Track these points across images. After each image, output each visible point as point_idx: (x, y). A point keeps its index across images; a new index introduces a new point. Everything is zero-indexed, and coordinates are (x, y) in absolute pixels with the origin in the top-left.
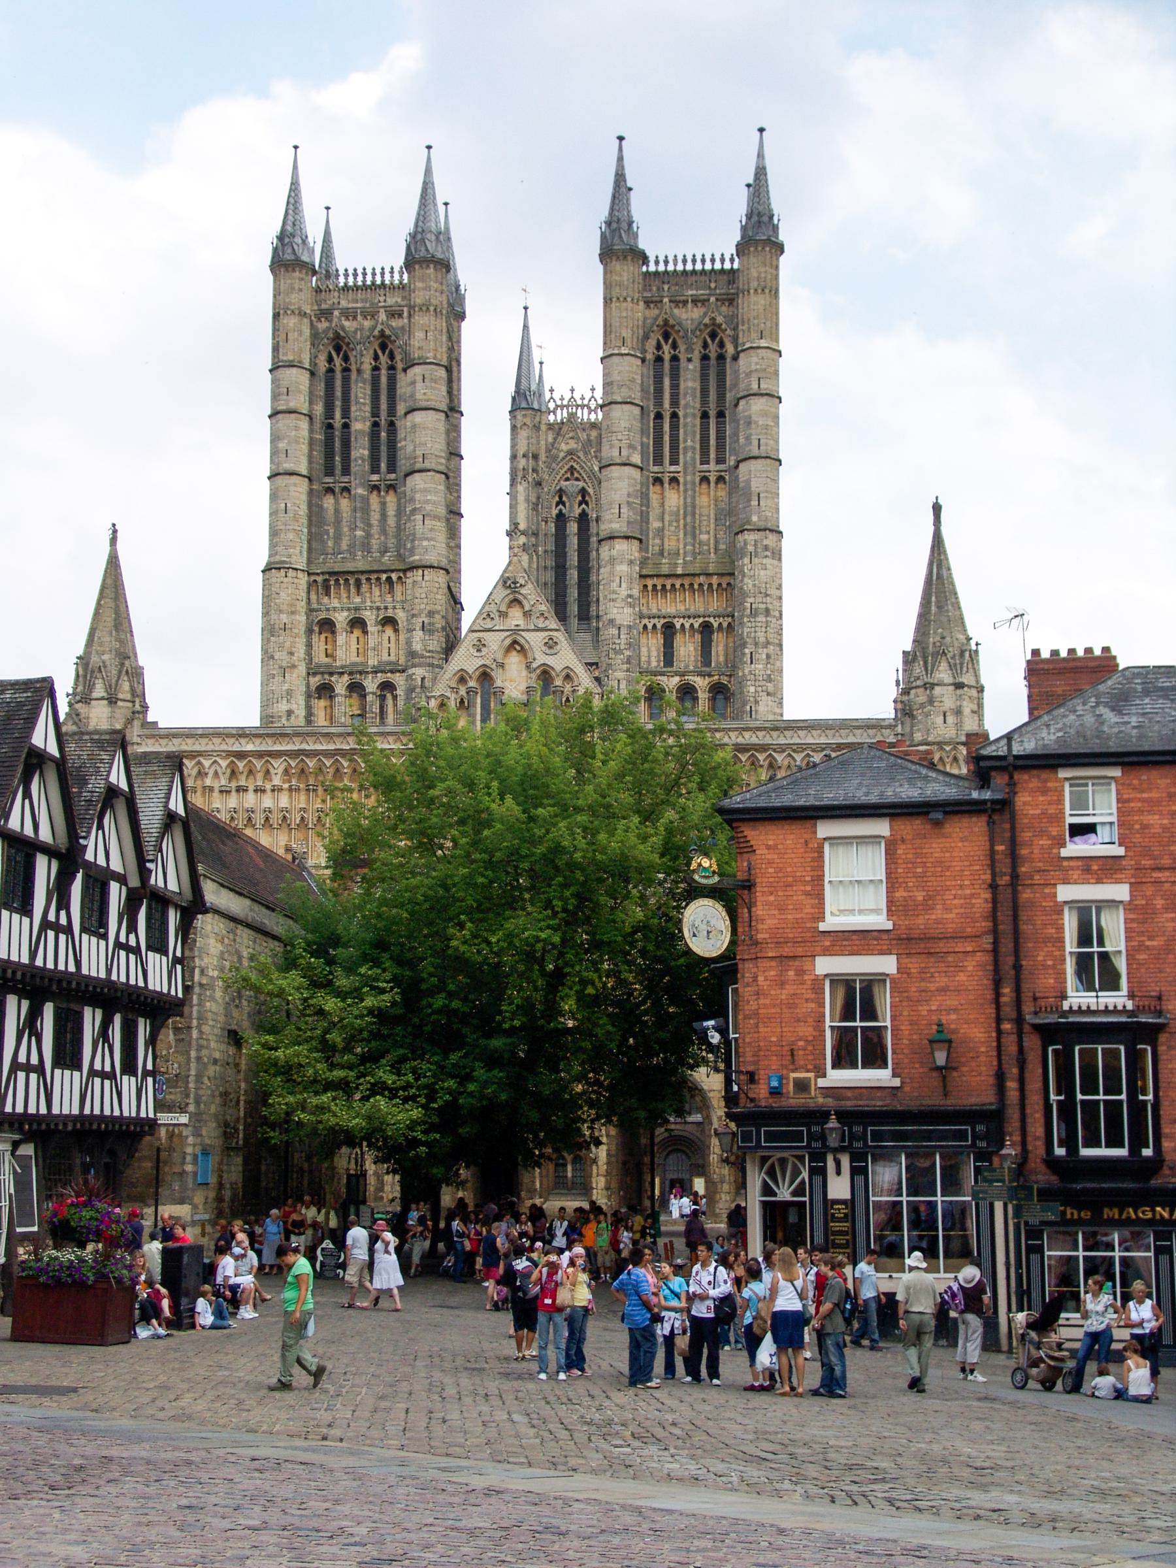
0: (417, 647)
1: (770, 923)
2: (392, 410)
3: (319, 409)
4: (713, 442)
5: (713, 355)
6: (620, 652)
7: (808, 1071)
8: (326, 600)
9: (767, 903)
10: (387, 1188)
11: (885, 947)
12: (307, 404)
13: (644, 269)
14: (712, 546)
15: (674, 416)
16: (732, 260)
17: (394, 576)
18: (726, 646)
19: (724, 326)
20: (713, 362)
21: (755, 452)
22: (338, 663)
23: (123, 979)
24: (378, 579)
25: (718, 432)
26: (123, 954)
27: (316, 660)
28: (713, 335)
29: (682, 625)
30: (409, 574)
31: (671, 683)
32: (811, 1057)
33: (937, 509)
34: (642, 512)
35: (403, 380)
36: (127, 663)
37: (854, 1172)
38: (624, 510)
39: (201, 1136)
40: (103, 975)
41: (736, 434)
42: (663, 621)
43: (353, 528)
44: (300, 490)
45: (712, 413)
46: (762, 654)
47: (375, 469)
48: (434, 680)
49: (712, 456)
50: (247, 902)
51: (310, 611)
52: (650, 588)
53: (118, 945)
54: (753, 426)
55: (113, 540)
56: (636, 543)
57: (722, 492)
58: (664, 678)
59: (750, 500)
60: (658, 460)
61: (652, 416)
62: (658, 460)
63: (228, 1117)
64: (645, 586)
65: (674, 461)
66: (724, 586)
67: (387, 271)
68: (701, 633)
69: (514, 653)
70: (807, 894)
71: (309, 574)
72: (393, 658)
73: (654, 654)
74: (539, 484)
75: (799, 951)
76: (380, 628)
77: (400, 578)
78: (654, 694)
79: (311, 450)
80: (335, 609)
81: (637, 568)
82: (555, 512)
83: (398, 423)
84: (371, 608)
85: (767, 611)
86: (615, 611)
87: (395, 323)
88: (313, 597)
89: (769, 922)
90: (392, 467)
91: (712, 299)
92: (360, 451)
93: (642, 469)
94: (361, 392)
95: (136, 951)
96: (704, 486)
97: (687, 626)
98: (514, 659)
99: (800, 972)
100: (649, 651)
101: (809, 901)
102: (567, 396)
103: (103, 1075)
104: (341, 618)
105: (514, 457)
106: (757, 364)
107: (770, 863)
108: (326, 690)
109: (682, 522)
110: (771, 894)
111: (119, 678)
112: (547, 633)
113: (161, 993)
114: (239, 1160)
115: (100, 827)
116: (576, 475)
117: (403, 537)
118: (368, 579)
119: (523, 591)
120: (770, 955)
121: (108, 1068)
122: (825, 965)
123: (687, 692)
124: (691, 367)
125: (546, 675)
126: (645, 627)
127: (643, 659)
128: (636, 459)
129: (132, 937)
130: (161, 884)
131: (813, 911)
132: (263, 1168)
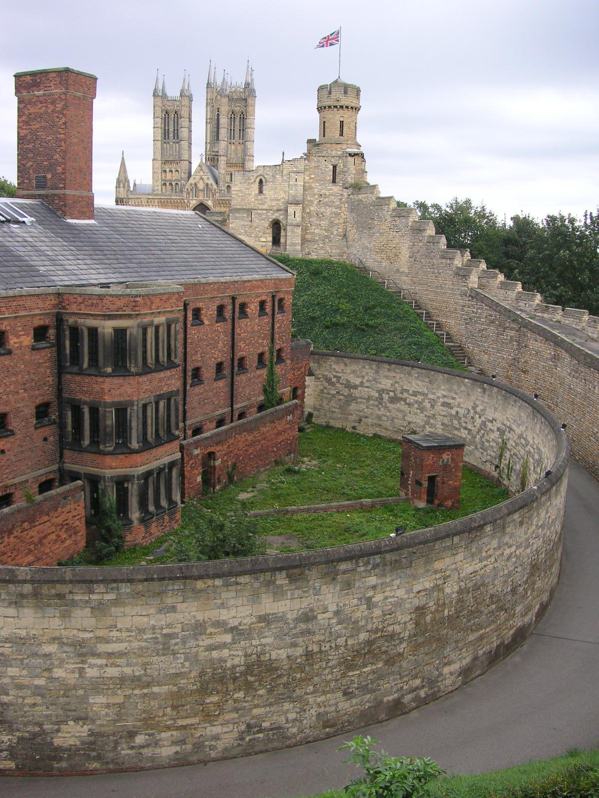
0: (182, 176)
2: (177, 127)
3: (163, 126)
33: (283, 153)
35: (180, 120)
43: (170, 151)
47: (174, 139)
48: (186, 183)
51: (162, 168)
55: (123, 154)
57: (243, 146)
60: (231, 139)
62: (231, 139)
87: (178, 108)
90: (177, 138)
92: (171, 135)
94: (171, 123)
98: (201, 181)
104: (168, 170)
108: (165, 184)
117: (180, 154)
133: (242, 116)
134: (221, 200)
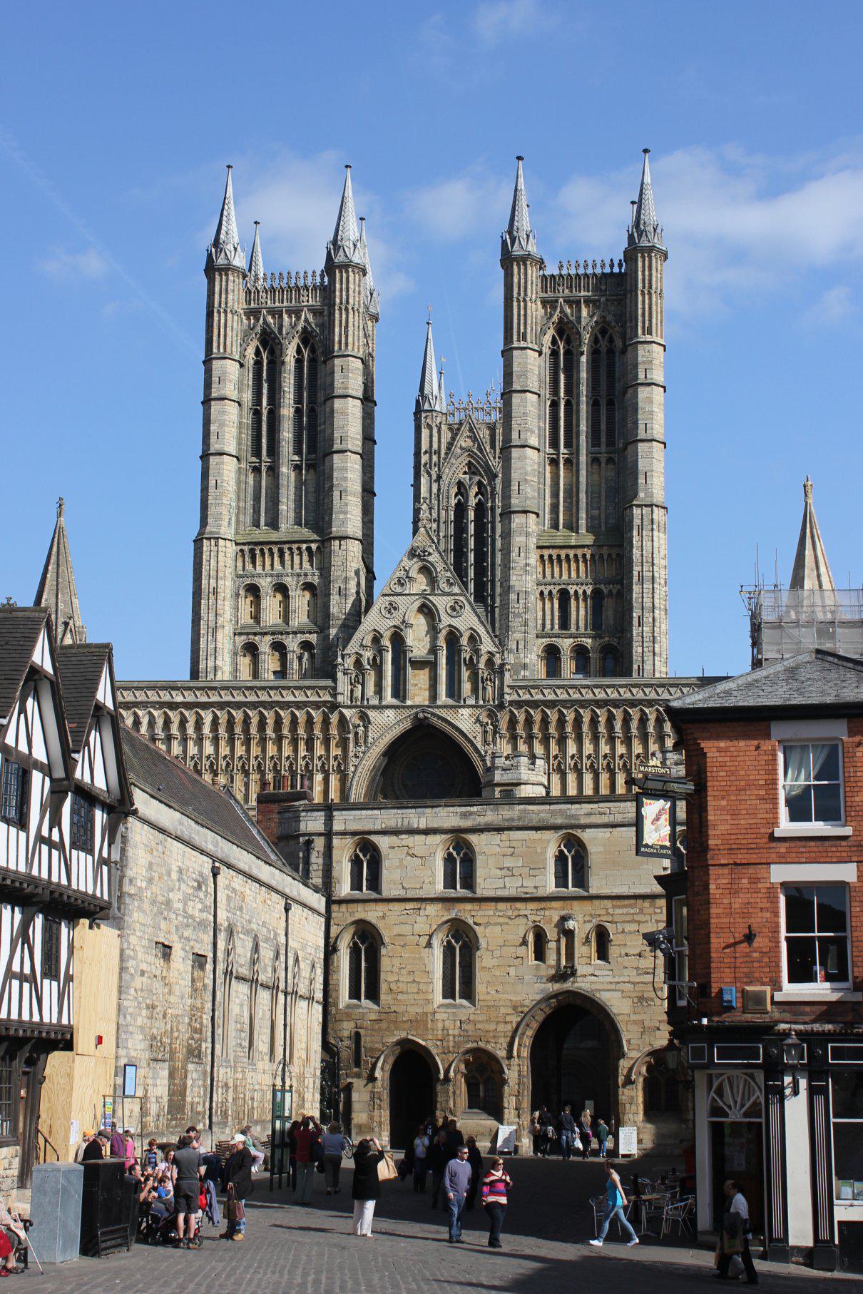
1: (722, 828)
3: (247, 397)
4: (603, 427)
5: (604, 349)
7: (763, 984)
8: (249, 567)
9: (717, 808)
10: (308, 1105)
11: (844, 854)
12: (236, 392)
13: (541, 272)
14: (603, 520)
15: (568, 404)
16: (620, 265)
17: (314, 546)
19: (612, 324)
20: (604, 355)
23: (45, 875)
24: (299, 549)
26: (45, 848)
27: (242, 622)
28: (603, 331)
29: (576, 592)
31: (566, 644)
32: (767, 970)
34: (539, 489)
36: (71, 623)
37: (812, 1091)
39: (126, 1048)
40: (22, 868)
41: (624, 420)
42: (558, 588)
44: (230, 468)
45: (603, 402)
46: (648, 618)
47: (298, 451)
49: (603, 439)
50: (178, 815)
52: (546, 558)
53: (41, 839)
54: (640, 412)
56: (534, 516)
58: (557, 639)
59: (637, 479)
61: (548, 403)
62: (554, 443)
63: (155, 1031)
66: (614, 557)
67: (310, 275)
70: (762, 799)
71: (237, 544)
73: (548, 617)
74: (439, 477)
75: (753, 858)
76: (299, 592)
77: (318, 548)
78: (552, 654)
79: (240, 433)
80: (259, 576)
81: (535, 540)
82: (453, 502)
83: (318, 410)
85: (653, 576)
88: (240, 564)
89: (721, 827)
91: (603, 299)
93: (539, 450)
95: (60, 846)
97: (580, 592)
99: (755, 881)
101: (764, 806)
102: (465, 400)
103: (22, 978)
104: (265, 584)
105: (417, 454)
106: (643, 356)
107: (722, 766)
108: (251, 649)
109: (574, 499)
110: (723, 798)
111: (64, 635)
112: (453, 598)
113: (86, 894)
114: (166, 1073)
115: (23, 710)
116: (473, 469)
118: (290, 549)
119: (430, 559)
120: (723, 862)
121: (27, 970)
122: (781, 873)
123: (580, 652)
126: (542, 593)
128: (533, 441)
129: (55, 831)
130: (87, 779)
131: (767, 816)
132: (189, 1082)
133: (604, 345)
134: (519, 704)
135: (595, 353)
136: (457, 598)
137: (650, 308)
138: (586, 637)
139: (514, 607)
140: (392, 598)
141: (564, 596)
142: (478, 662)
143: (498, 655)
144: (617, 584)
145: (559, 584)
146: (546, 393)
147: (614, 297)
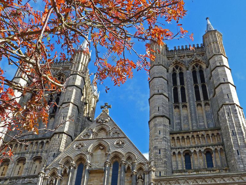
6: (161, 159)
17: (45, 141)
18: (221, 159)
21: (223, 82)
22: (6, 176)
24: (37, 143)
25: (203, 90)
29: (195, 151)
30: (52, 139)
38: (161, 108)
42: (184, 150)
61: (173, 89)
64: (173, 138)
65: (184, 100)
66: (215, 134)
68: (206, 154)
69: (99, 151)
72: (35, 174)
73: (180, 164)
76: (33, 161)
77: (47, 142)
84: (30, 153)
86: (157, 143)
96: (199, 107)
97: (197, 150)
98: (99, 152)
100: (177, 163)
106: (218, 59)
112: (118, 139)
118: (32, 143)
124: (188, 71)
125: (116, 156)
126: (174, 153)
127: (174, 167)
133: (197, 69)
135: (194, 73)
136: (120, 139)
137: (218, 47)
138: (204, 171)
139: (157, 156)
140: (81, 142)
141: (187, 155)
142: (133, 169)
143: (147, 165)
144: (219, 145)
145: (184, 148)
146: (171, 84)
147: (201, 53)
